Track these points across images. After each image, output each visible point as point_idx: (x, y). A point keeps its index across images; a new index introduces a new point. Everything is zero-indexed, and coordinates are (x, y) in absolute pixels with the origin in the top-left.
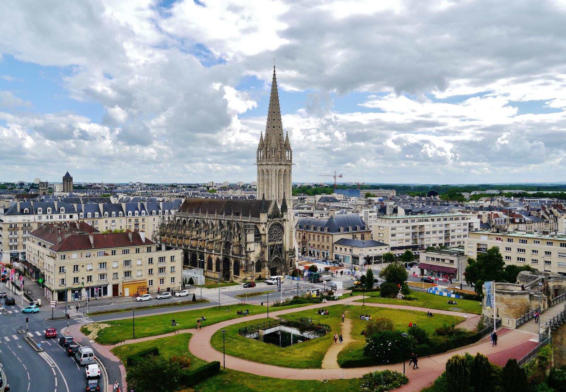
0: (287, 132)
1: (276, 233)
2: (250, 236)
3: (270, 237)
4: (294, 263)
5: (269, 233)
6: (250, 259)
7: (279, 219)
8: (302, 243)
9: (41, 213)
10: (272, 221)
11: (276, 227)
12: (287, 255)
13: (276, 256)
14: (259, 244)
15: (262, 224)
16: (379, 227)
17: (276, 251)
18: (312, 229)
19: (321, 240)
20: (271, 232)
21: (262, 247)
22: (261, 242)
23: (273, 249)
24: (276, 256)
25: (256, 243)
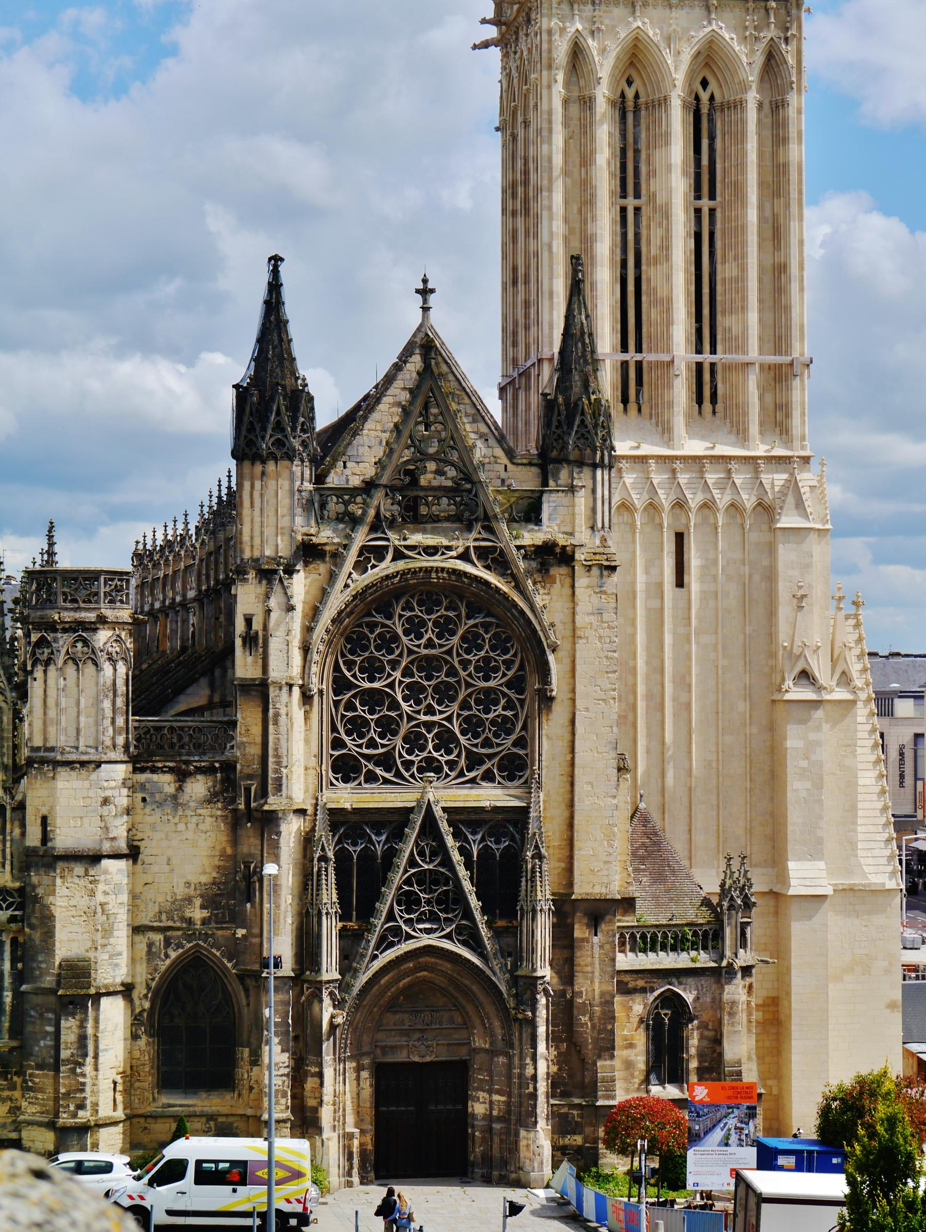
1: (445, 693)
2: (52, 693)
3: (357, 727)
4: (716, 1041)
5: (340, 685)
6: (49, 934)
7: (468, 541)
10: (379, 553)
11: (445, 628)
14: (198, 787)
15: (241, 572)
20: (372, 670)
21: (235, 823)
22: (229, 767)
23: (391, 854)
25: (166, 782)
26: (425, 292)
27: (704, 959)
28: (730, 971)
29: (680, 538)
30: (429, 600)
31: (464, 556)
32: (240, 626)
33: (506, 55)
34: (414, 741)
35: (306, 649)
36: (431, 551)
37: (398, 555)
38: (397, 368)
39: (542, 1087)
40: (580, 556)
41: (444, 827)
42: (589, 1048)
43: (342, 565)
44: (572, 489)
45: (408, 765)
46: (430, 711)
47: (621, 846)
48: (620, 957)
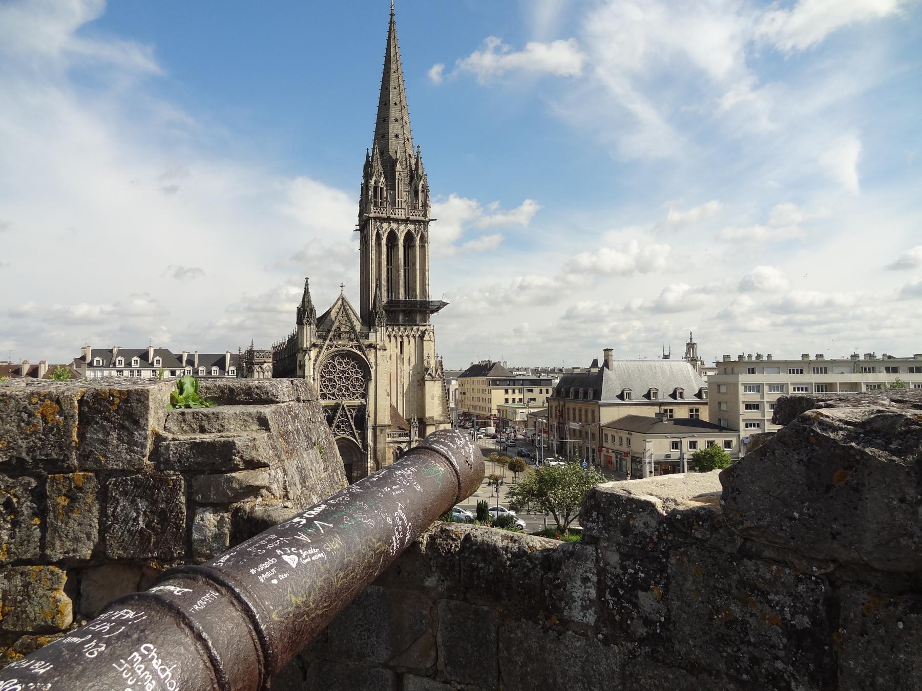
0: (418, 147)
1: (348, 378)
3: (326, 386)
5: (322, 377)
8: (559, 428)
9: (123, 366)
10: (331, 346)
11: (347, 363)
12: (380, 438)
13: (342, 436)
15: (298, 350)
16: (719, 386)
17: (342, 422)
18: (572, 395)
19: (583, 418)
20: (330, 373)
24: (342, 435)
26: (342, 286)
27: (407, 438)
28: (413, 441)
29: (402, 343)
30: (343, 357)
31: (352, 347)
32: (298, 363)
33: (361, 233)
34: (340, 390)
35: (314, 369)
36: (345, 346)
37: (336, 347)
38: (336, 304)
39: (369, 469)
40: (378, 347)
41: (346, 409)
42: (380, 461)
43: (322, 349)
44: (376, 332)
45: (338, 395)
46: (343, 383)
47: (388, 413)
48: (387, 439)
